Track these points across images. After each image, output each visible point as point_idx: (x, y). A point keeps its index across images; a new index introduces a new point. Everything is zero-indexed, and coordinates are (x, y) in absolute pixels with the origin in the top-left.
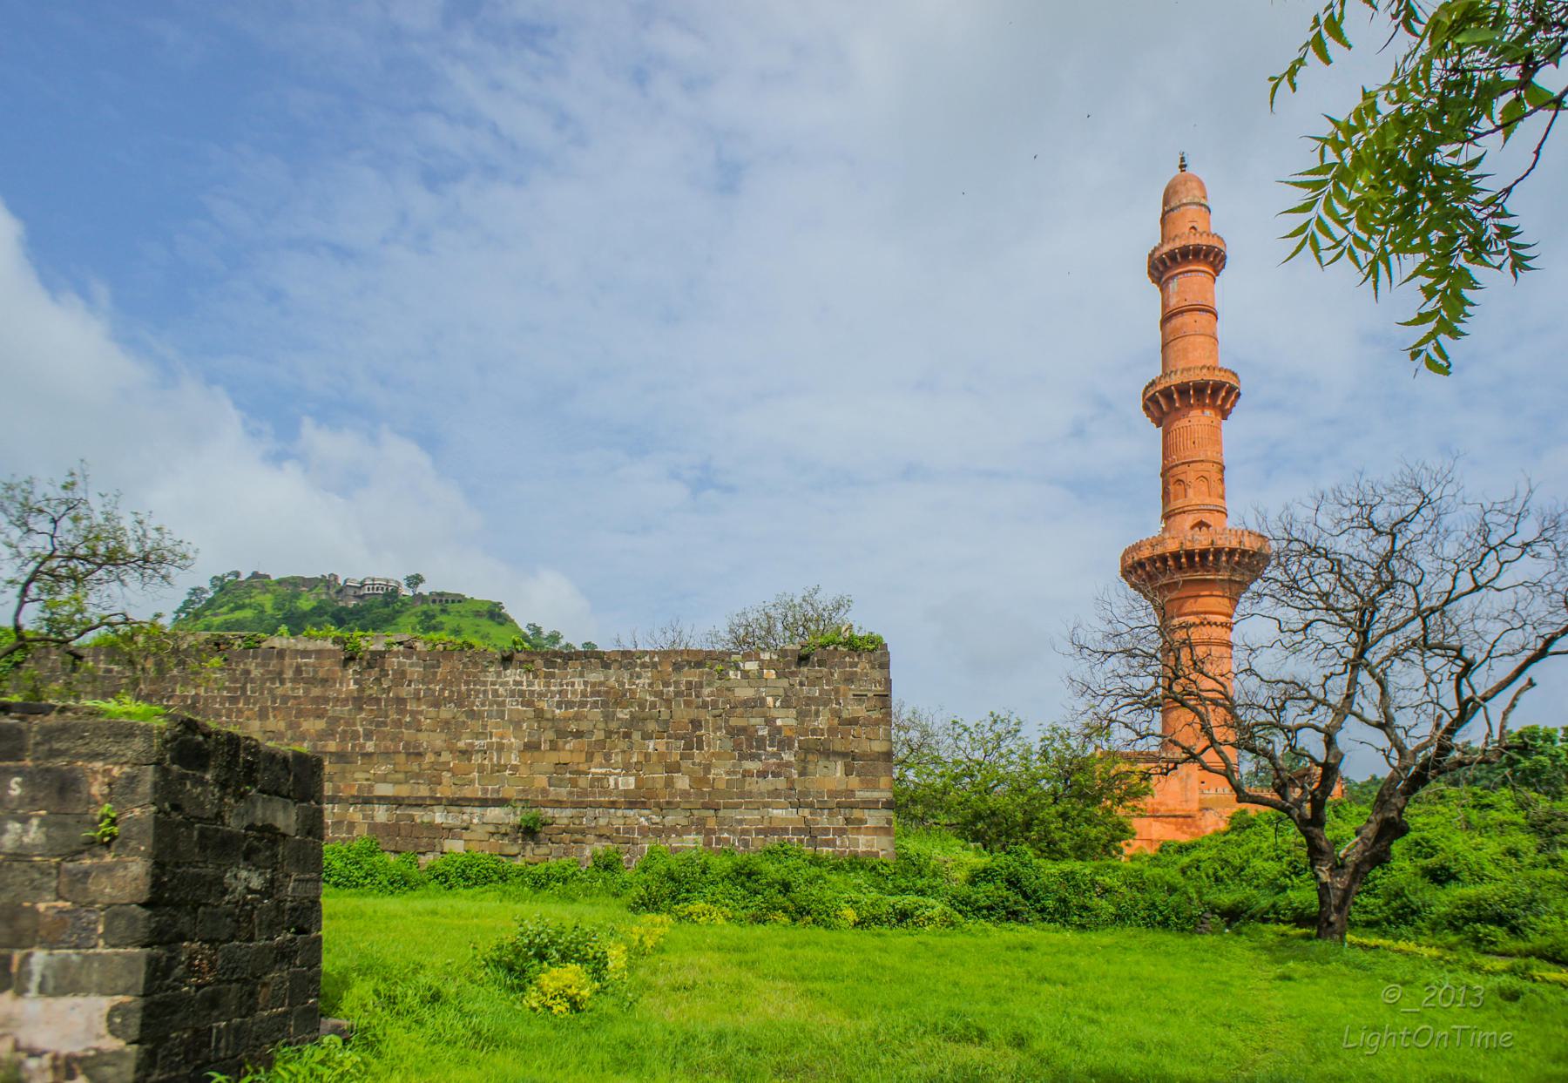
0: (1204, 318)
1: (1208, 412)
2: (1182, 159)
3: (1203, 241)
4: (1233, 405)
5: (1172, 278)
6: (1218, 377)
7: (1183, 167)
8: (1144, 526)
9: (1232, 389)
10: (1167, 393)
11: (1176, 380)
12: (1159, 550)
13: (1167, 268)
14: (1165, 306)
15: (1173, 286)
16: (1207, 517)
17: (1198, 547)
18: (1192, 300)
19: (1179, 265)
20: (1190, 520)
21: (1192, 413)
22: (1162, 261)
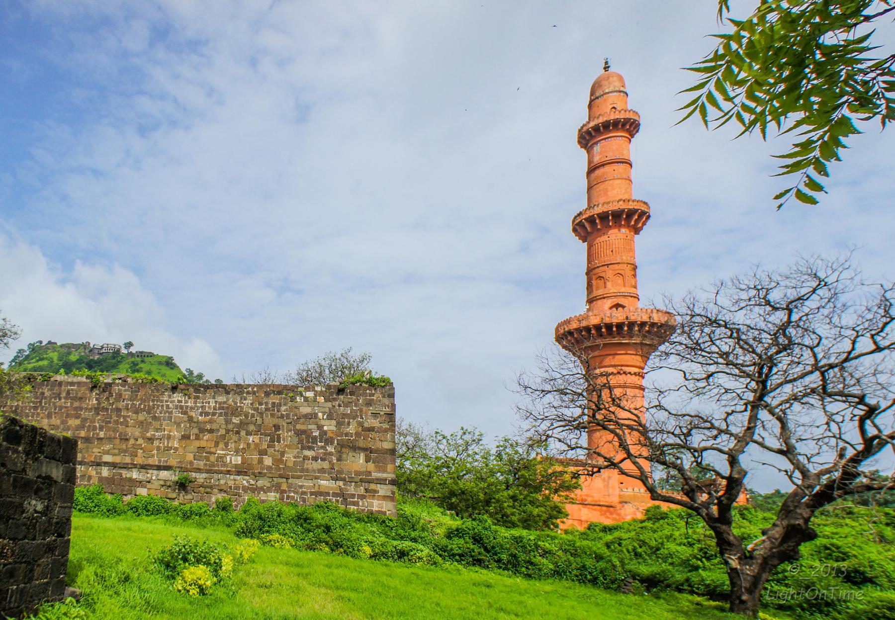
0: (622, 166)
1: (623, 230)
2: (606, 63)
3: (621, 116)
4: (644, 224)
5: (596, 143)
6: (632, 206)
7: (606, 68)
8: (575, 307)
9: (643, 213)
10: (591, 220)
11: (598, 210)
12: (584, 324)
13: (588, 141)
14: (590, 162)
15: (597, 149)
16: (622, 301)
17: (615, 321)
18: (611, 156)
19: (601, 134)
20: (608, 303)
21: (610, 232)
22: (588, 133)
